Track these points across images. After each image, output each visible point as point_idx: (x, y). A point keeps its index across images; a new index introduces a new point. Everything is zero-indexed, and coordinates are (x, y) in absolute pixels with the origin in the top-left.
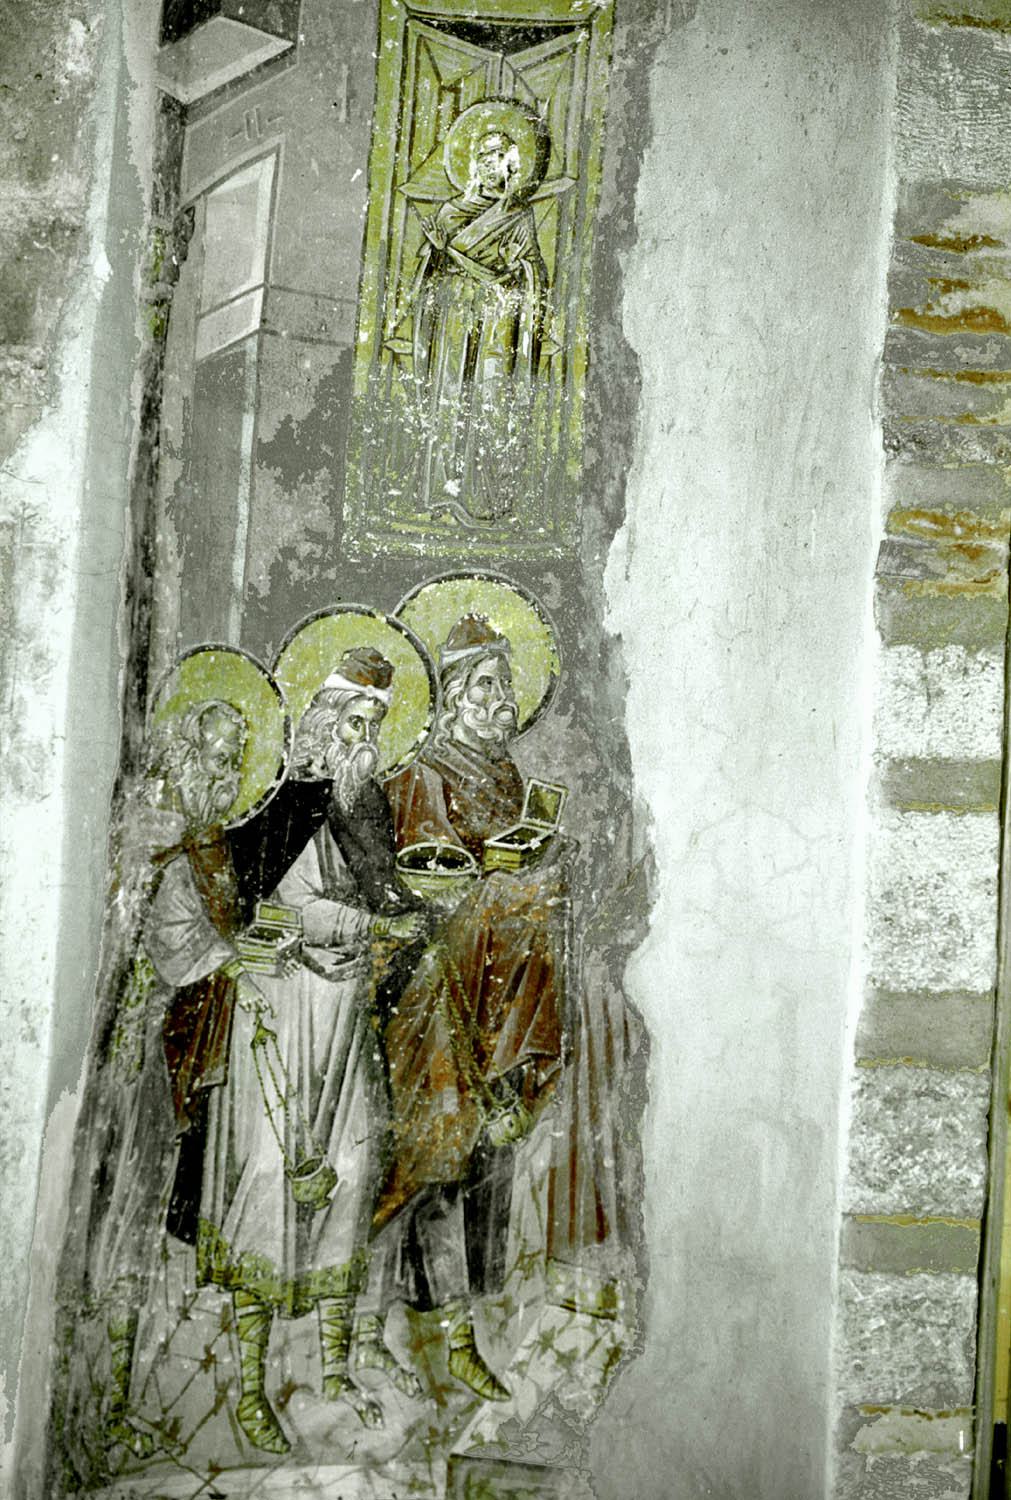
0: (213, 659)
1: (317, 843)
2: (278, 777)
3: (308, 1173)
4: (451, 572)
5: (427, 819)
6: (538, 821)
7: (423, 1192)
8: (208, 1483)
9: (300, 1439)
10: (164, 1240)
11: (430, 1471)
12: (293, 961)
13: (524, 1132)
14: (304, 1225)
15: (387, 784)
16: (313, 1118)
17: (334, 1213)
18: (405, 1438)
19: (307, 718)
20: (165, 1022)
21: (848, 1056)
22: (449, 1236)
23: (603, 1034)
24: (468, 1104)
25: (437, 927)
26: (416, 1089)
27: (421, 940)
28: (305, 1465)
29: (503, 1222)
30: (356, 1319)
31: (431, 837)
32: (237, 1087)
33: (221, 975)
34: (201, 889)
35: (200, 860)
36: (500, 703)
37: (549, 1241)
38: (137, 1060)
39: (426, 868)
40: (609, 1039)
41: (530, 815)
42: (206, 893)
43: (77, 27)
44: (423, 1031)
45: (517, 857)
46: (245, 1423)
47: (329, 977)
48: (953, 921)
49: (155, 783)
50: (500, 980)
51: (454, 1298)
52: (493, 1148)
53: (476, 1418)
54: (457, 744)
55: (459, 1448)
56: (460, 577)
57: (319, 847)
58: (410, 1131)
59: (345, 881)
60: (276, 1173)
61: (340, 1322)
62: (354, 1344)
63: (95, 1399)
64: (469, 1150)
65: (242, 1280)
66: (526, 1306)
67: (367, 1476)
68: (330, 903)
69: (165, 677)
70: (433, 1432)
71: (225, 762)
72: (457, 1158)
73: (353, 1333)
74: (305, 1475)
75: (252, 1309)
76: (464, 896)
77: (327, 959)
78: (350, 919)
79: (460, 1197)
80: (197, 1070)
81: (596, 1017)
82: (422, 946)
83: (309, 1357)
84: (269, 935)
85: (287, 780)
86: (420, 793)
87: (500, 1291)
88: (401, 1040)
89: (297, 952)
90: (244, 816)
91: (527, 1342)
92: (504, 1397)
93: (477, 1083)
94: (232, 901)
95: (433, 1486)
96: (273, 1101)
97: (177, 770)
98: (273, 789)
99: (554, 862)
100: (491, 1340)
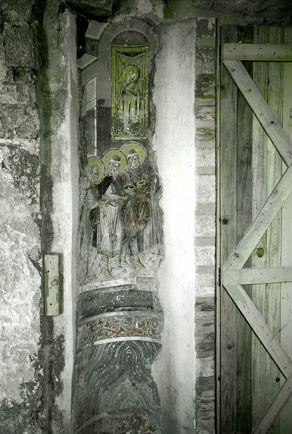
13: (145, 228)
21: (194, 213)
25: (130, 198)
29: (143, 241)
33: (98, 207)
43: (63, 57)
48: (209, 192)
54: (131, 169)
59: (115, 191)
77: (113, 203)
78: (117, 197)
80: (95, 222)
86: (126, 177)
89: (109, 203)
93: (137, 221)
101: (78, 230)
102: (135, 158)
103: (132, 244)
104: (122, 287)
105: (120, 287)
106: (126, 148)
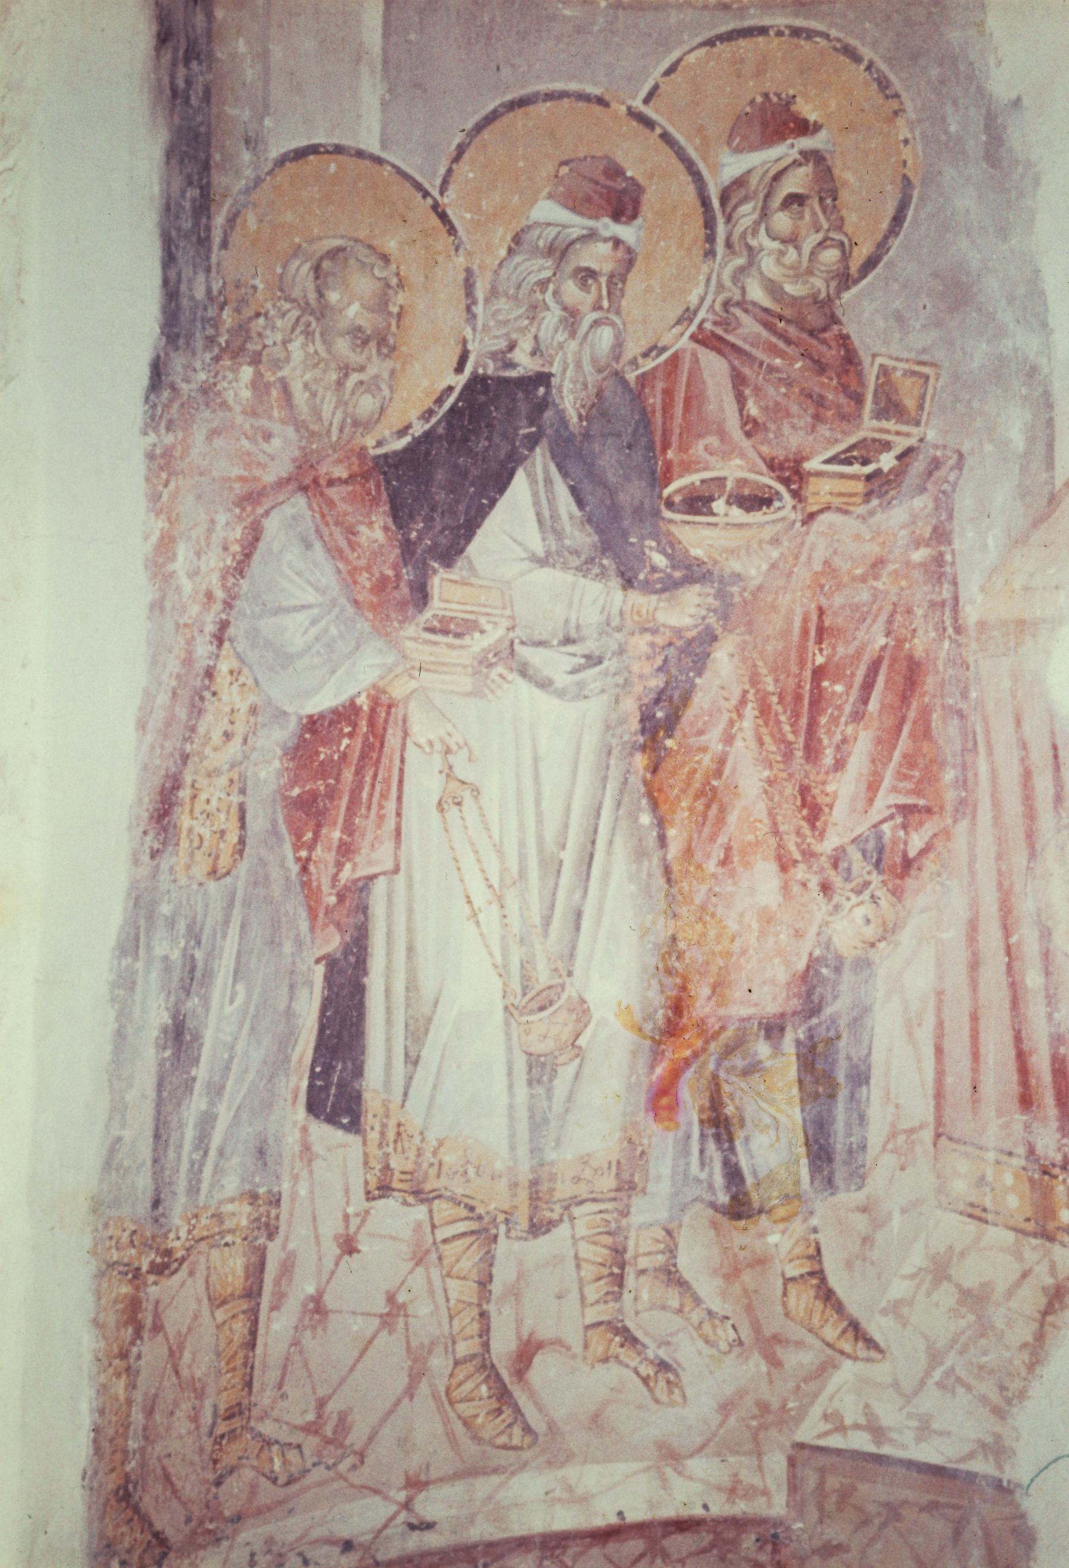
0: (333, 167)
1: (532, 477)
3: (542, 1008)
4: (731, 26)
5: (708, 433)
6: (891, 425)
8: (407, 1505)
9: (552, 1426)
10: (304, 1130)
11: (760, 1468)
13: (888, 931)
14: (540, 1090)
15: (643, 379)
16: (547, 921)
19: (504, 273)
20: (280, 774)
24: (796, 889)
25: (734, 607)
27: (708, 627)
28: (562, 1465)
29: (860, 1077)
30: (633, 1234)
31: (712, 460)
32: (417, 876)
34: (335, 553)
35: (331, 504)
36: (820, 236)
37: (939, 1108)
38: (233, 838)
39: (713, 514)
41: (878, 415)
42: (347, 561)
44: (718, 773)
45: (859, 487)
46: (461, 1407)
47: (561, 694)
49: (235, 370)
50: (839, 688)
52: (840, 958)
53: (830, 1389)
59: (583, 539)
61: (608, 1240)
63: (186, 1406)
64: (801, 965)
65: (443, 1182)
66: (903, 1211)
69: (248, 191)
70: (764, 1407)
71: (365, 342)
73: (628, 1256)
75: (462, 1227)
76: (775, 554)
77: (555, 663)
78: (597, 598)
80: (346, 851)
82: (711, 638)
83: (559, 1297)
87: (860, 1188)
88: (684, 791)
90: (402, 432)
91: (907, 1269)
92: (873, 1354)
93: (809, 855)
94: (390, 573)
95: (765, 1493)
96: (480, 896)
97: (278, 352)
98: (450, 389)
99: (922, 490)
100: (849, 1265)
101: (130, 945)
102: (793, 184)
105: (611, 1547)
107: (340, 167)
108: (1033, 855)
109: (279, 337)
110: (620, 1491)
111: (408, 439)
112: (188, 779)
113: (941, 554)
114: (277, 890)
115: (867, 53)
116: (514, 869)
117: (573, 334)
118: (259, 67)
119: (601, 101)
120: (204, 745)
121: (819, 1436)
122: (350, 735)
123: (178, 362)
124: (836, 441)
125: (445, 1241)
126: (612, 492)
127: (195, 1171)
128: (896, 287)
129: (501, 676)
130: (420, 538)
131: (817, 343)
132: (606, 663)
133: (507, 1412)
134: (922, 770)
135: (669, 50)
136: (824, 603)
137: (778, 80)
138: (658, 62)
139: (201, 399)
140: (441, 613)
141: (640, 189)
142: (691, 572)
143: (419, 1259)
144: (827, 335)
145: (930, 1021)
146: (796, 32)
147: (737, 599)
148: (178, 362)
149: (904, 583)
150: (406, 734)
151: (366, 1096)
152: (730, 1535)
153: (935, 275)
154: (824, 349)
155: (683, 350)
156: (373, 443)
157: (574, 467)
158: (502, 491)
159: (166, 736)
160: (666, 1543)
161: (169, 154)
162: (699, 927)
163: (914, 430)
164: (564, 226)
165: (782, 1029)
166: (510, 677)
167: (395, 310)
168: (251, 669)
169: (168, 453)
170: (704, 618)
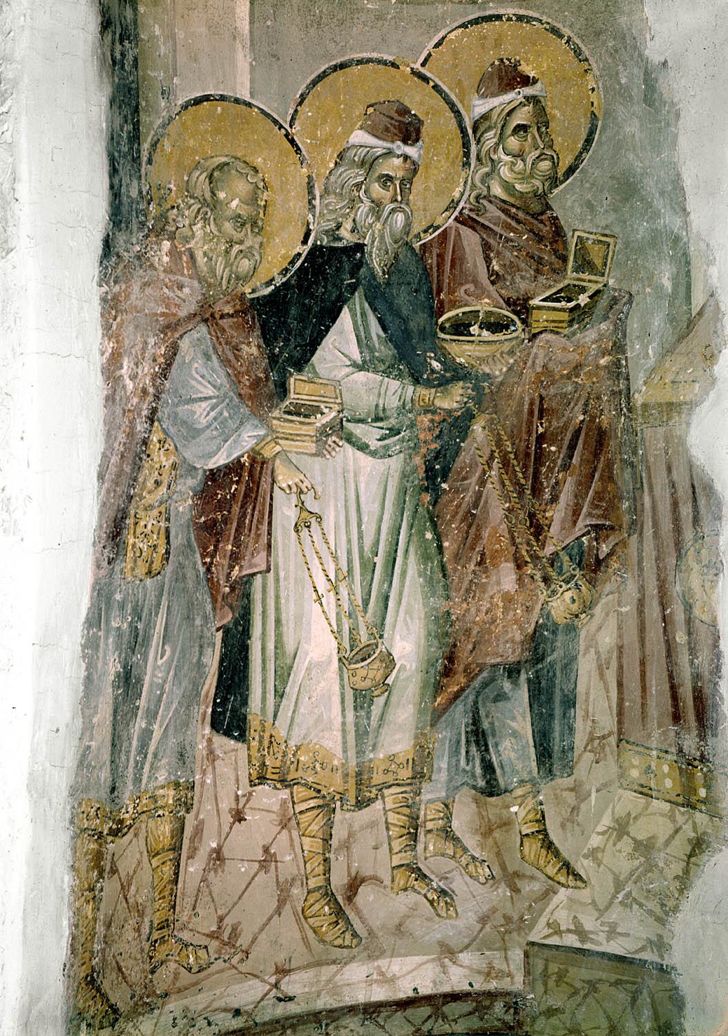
1: (350, 311)
2: (305, 242)
3: (364, 660)
4: (476, 16)
6: (586, 276)
7: (485, 674)
8: (276, 985)
9: (371, 932)
10: (210, 741)
12: (334, 438)
13: (587, 607)
16: (366, 602)
17: (393, 699)
18: (479, 926)
19: (332, 179)
22: (513, 718)
23: (668, 502)
25: (485, 396)
26: (472, 567)
27: (468, 410)
28: (377, 958)
29: (570, 702)
30: (423, 807)
32: (282, 574)
34: (225, 362)
35: (223, 330)
36: (538, 153)
37: (620, 722)
40: (675, 505)
41: (576, 270)
44: (476, 506)
45: (565, 316)
47: (373, 454)
49: (159, 244)
50: (553, 449)
51: (522, 782)
52: (556, 624)
53: (551, 907)
55: (535, 936)
56: (488, 19)
57: (354, 316)
58: (468, 610)
59: (385, 351)
60: (330, 662)
61: (407, 811)
62: (421, 831)
64: (530, 630)
65: (300, 773)
67: (443, 966)
68: (371, 375)
69: (164, 126)
70: (508, 919)
71: (243, 225)
72: (518, 637)
74: (379, 967)
75: (312, 803)
76: (511, 361)
77: (370, 434)
78: (394, 392)
79: (523, 677)
80: (235, 558)
81: (660, 480)
82: (469, 416)
83: (376, 848)
84: (304, 411)
85: (315, 245)
88: (453, 517)
89: (338, 429)
90: (269, 283)
91: (600, 828)
92: (579, 884)
93: (535, 558)
94: (262, 375)
95: (510, 975)
96: (322, 586)
97: (186, 231)
98: (299, 255)
99: (606, 318)
100: (563, 826)
101: (95, 620)
102: (521, 117)
103: (493, 716)
104: (426, 1011)
106: (455, 54)
107: (223, 109)
108: (679, 557)
109: (187, 222)
110: (414, 975)
111: (273, 287)
112: (132, 512)
113: (619, 360)
114: (190, 584)
115: (566, 32)
116: (345, 569)
117: (378, 218)
118: (170, 44)
119: (394, 65)
120: (142, 490)
121: (544, 938)
122: (237, 482)
123: (121, 238)
124: (550, 286)
125: (301, 812)
126: (405, 321)
127: (139, 767)
128: (587, 185)
129: (334, 442)
130: (280, 352)
131: (537, 222)
132: (403, 433)
133: (342, 923)
134: (607, 503)
135: (438, 31)
136: (544, 393)
137: (508, 51)
138: (431, 39)
139: (137, 262)
140: (295, 401)
141: (421, 122)
142: (456, 373)
143: (284, 825)
144: (543, 217)
145: (614, 664)
146: (520, 18)
147: (487, 391)
148: (121, 238)
149: (595, 380)
150: (274, 481)
151: (249, 717)
152: (487, 1003)
153: (612, 177)
154: (541, 226)
155: (451, 228)
156: (250, 291)
157: (380, 305)
158: (334, 322)
159: (117, 484)
160: (445, 1009)
161: (112, 102)
162: (465, 605)
163: (600, 279)
164: (372, 147)
165: (519, 672)
166: (341, 444)
167: (263, 203)
168: (172, 439)
169: (115, 298)
170: (466, 403)
